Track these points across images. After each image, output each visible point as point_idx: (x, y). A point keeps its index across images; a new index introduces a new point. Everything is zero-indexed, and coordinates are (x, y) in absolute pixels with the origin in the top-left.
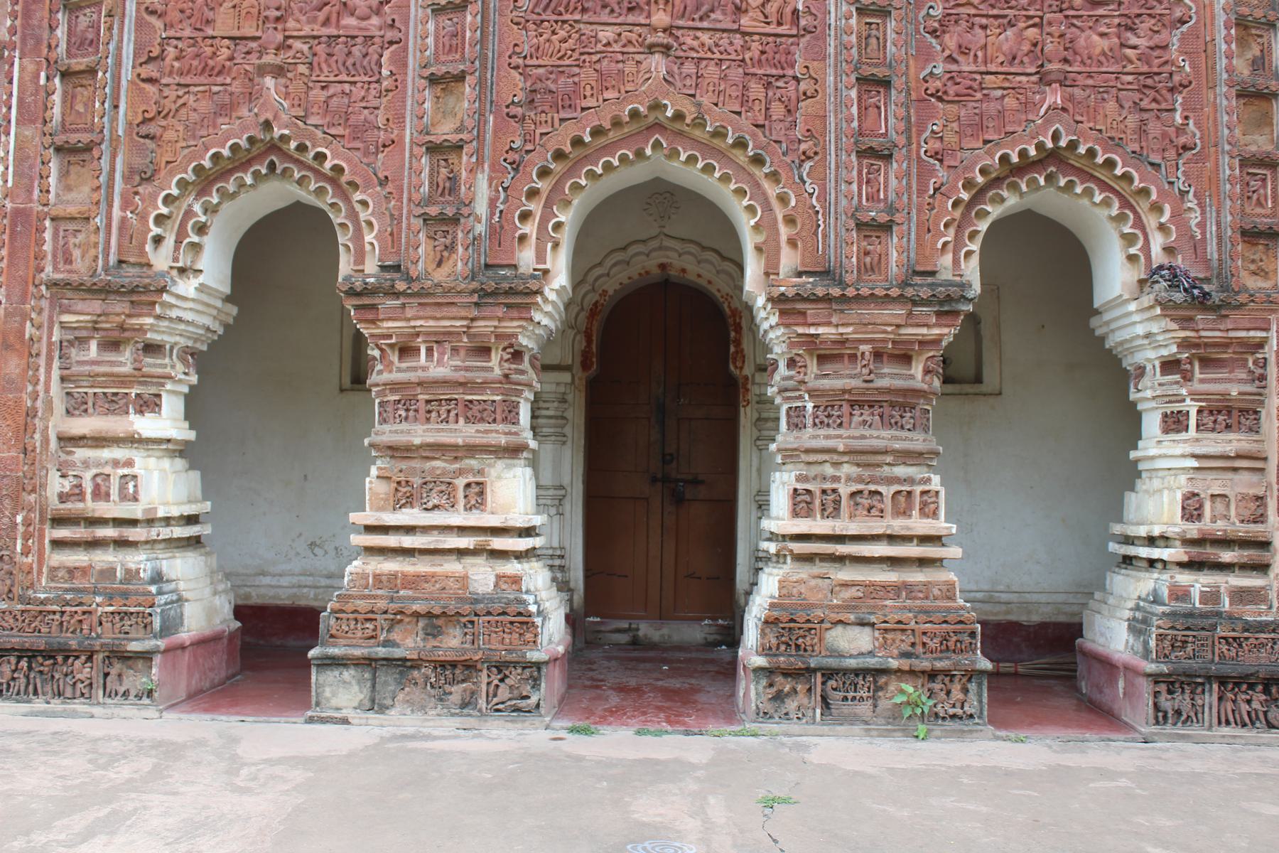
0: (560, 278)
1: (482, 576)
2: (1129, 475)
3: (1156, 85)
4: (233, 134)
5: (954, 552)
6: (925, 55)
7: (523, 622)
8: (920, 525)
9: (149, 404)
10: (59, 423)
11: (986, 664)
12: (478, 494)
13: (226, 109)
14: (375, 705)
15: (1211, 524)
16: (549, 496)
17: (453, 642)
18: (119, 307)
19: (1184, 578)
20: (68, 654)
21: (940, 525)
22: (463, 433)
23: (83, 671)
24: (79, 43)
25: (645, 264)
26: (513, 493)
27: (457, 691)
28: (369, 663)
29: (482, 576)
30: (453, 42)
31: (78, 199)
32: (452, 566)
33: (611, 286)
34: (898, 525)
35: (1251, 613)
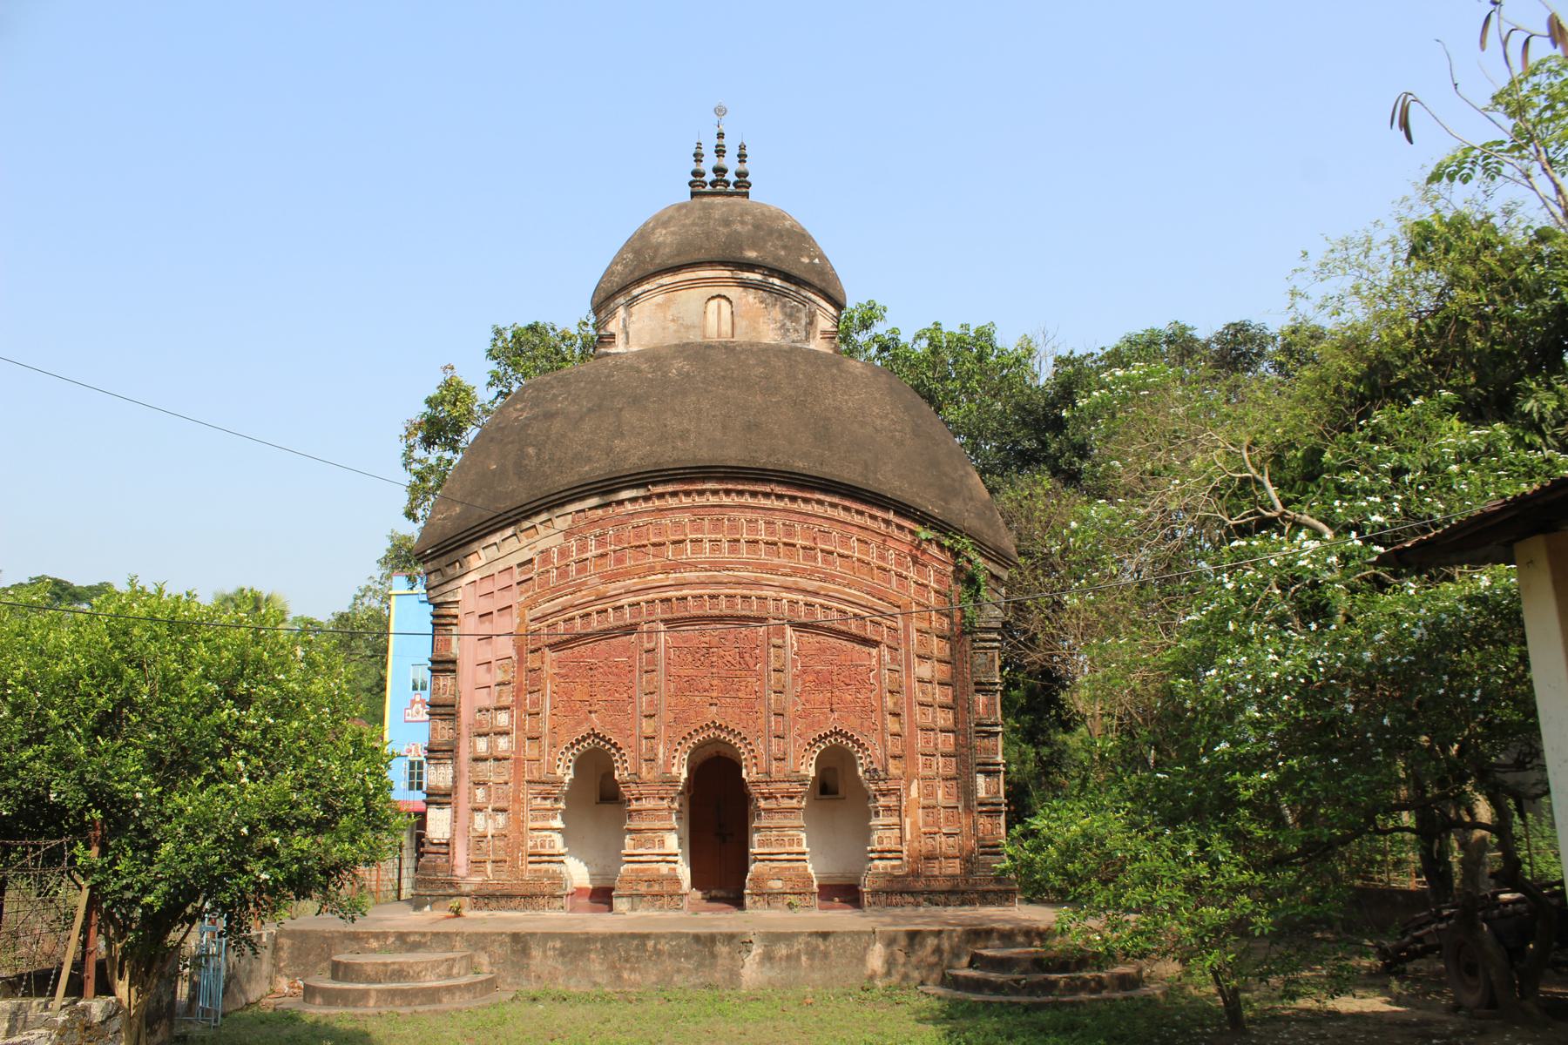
0: (685, 775)
1: (664, 869)
2: (869, 831)
3: (867, 710)
4: (584, 730)
5: (807, 857)
6: (795, 704)
7: (677, 881)
8: (796, 849)
9: (554, 817)
10: (531, 825)
11: (815, 888)
12: (662, 842)
13: (579, 724)
14: (633, 909)
15: (886, 846)
16: (680, 846)
17: (656, 888)
18: (548, 787)
19: (877, 862)
20: (536, 896)
21: (804, 848)
22: (657, 825)
23: (541, 901)
24: (533, 704)
25: (710, 751)
26: (672, 842)
27: (658, 903)
28: (630, 896)
29: (664, 869)
30: (650, 704)
31: (534, 754)
32: (655, 865)
33: (699, 761)
34: (789, 849)
35: (896, 873)
